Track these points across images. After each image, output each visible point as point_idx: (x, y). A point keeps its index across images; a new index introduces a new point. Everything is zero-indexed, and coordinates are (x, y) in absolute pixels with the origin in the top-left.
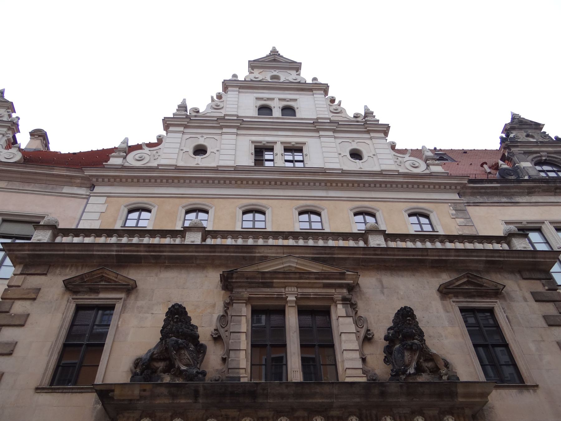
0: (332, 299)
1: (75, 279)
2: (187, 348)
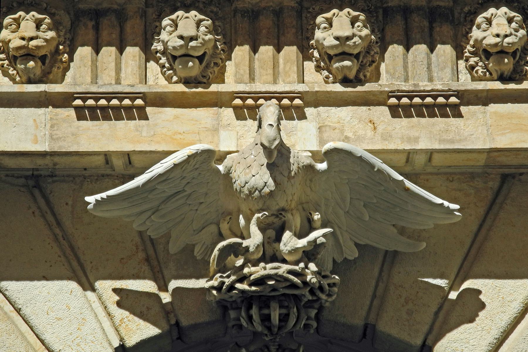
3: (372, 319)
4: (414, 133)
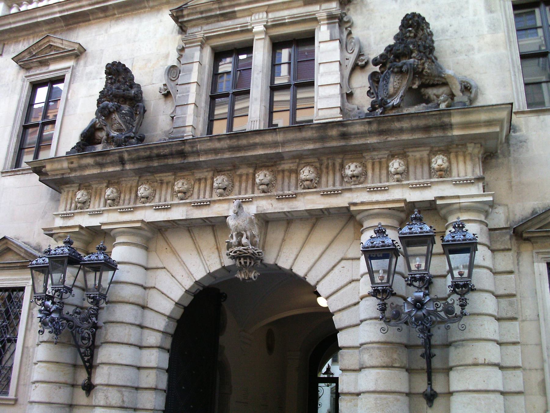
0: (315, 20)
1: (23, 55)
2: (118, 109)
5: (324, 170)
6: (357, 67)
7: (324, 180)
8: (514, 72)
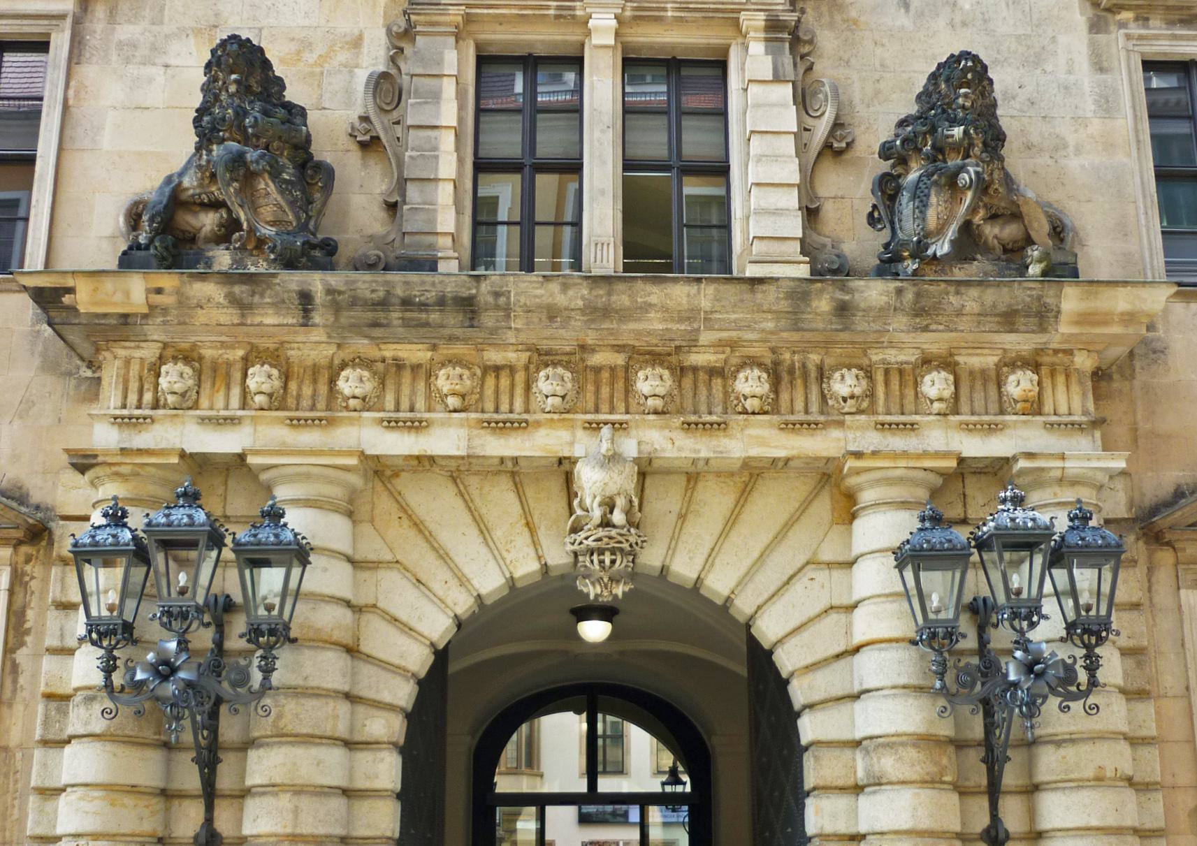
3: (667, 562)
4: (697, 447)
5: (786, 377)
6: (835, 149)
7: (785, 396)
8: (1145, 207)
